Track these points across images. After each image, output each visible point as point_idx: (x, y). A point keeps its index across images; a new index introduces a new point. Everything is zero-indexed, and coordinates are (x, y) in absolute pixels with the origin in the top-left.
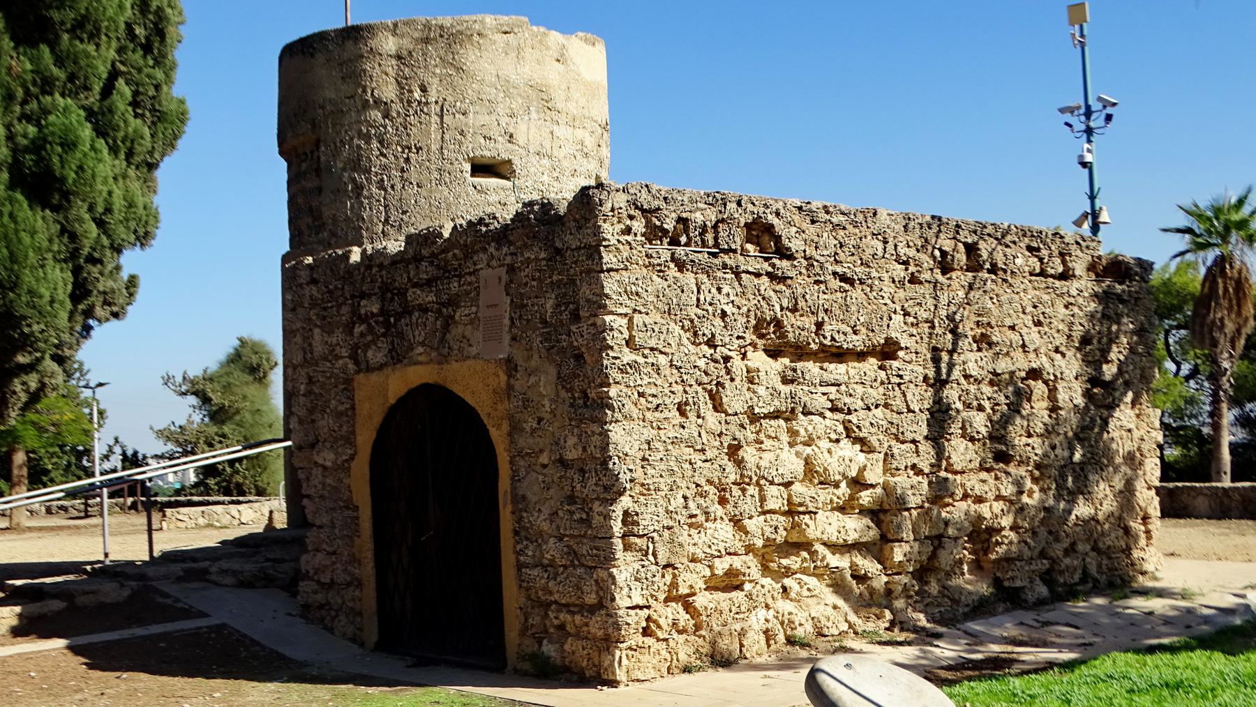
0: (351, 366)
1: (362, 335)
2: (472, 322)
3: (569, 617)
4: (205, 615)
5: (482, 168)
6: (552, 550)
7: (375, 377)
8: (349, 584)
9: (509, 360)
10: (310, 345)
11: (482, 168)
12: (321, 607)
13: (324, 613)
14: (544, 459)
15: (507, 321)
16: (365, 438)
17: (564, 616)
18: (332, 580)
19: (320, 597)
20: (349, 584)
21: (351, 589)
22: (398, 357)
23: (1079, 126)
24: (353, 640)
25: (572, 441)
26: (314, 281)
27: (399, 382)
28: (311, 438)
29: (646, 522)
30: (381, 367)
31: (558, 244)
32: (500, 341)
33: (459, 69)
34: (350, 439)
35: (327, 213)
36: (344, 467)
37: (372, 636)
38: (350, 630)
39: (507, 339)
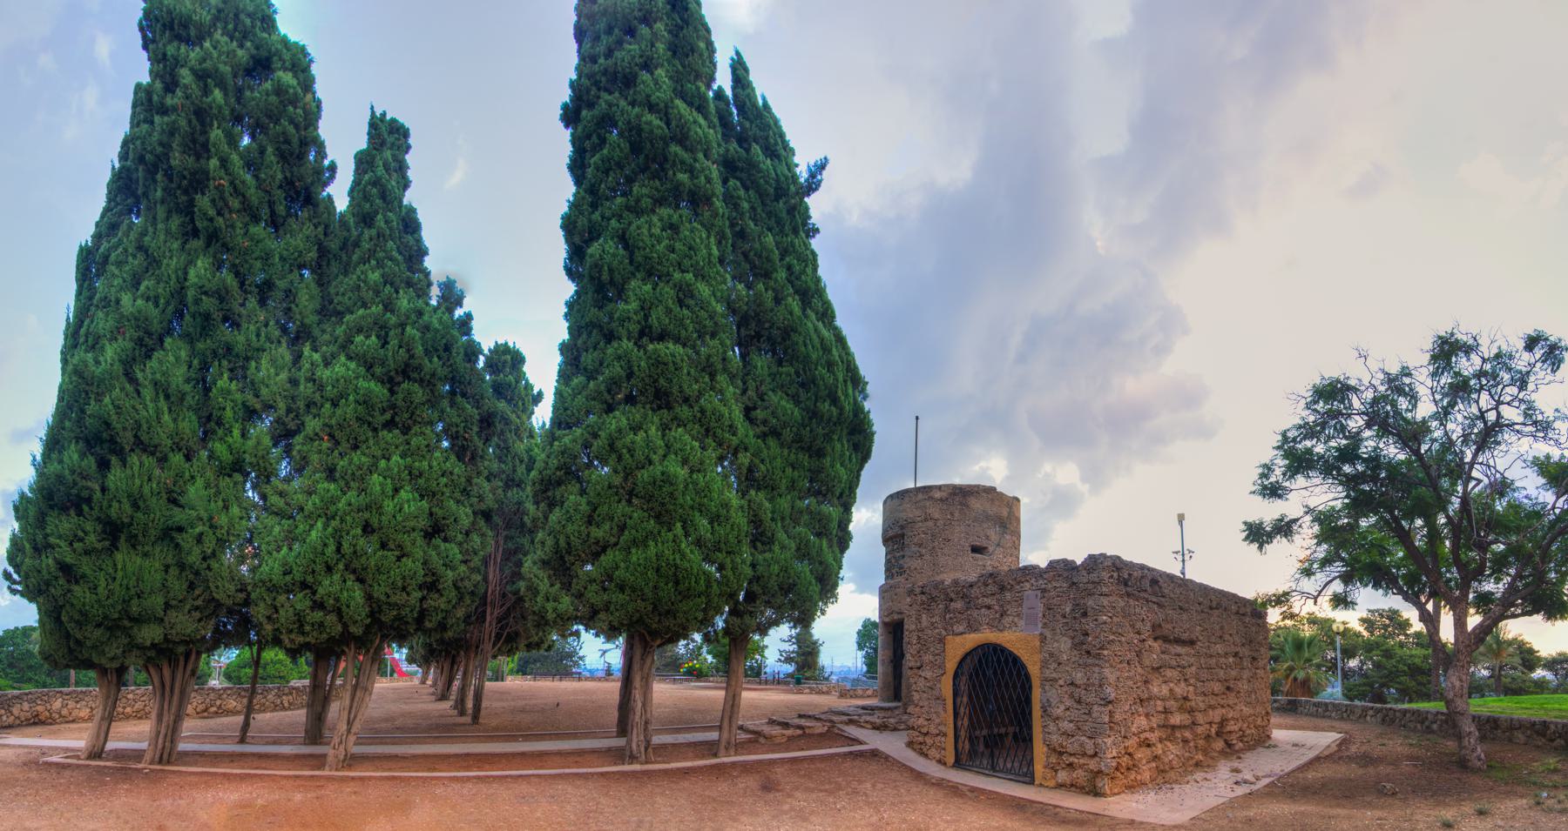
4: (861, 743)
5: (976, 550)
6: (1067, 726)
7: (958, 639)
11: (976, 550)
14: (1061, 682)
16: (951, 666)
17: (1072, 759)
19: (921, 739)
24: (939, 761)
27: (972, 640)
29: (1118, 717)
34: (942, 666)
36: (938, 679)
37: (951, 760)
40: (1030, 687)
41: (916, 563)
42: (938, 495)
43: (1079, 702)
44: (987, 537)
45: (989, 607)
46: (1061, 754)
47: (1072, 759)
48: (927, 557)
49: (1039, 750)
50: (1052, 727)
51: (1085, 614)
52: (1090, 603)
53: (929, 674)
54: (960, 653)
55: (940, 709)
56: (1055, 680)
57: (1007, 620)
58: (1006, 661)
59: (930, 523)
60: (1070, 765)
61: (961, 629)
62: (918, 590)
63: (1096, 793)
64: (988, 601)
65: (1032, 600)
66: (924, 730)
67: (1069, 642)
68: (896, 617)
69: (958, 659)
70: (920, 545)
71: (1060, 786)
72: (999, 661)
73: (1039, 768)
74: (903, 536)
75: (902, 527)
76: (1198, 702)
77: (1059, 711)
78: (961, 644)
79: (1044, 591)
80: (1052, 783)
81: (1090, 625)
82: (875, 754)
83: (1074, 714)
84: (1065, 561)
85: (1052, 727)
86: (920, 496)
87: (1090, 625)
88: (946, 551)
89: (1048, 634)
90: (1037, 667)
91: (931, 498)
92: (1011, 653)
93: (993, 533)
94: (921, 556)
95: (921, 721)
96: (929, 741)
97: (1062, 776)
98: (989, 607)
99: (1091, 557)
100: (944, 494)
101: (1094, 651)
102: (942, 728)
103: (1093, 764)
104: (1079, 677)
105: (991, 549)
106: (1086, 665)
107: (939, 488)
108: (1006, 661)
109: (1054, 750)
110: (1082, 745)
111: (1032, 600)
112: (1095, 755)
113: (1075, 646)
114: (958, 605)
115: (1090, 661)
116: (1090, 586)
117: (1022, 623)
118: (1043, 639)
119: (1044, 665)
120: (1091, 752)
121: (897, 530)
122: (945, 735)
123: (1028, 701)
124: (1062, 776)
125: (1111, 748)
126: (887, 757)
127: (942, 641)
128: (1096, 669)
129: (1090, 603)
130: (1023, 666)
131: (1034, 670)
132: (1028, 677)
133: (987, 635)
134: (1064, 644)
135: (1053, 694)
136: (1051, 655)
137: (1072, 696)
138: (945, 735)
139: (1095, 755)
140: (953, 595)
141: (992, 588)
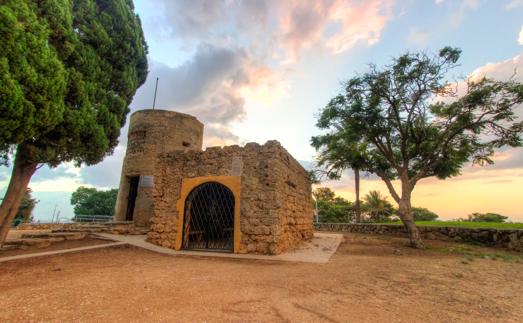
0: (181, 177)
1: (187, 169)
2: (229, 168)
3: (259, 238)
6: (254, 220)
7: (191, 180)
8: (170, 232)
9: (242, 176)
10: (165, 172)
12: (157, 238)
13: (158, 240)
14: (252, 199)
15: (242, 167)
16: (184, 194)
18: (164, 231)
19: (158, 236)
20: (170, 232)
21: (171, 233)
22: (199, 174)
24: (170, 247)
25: (262, 195)
26: (168, 157)
28: (161, 194)
30: (193, 177)
31: (261, 151)
32: (239, 172)
33: (183, 123)
35: (145, 147)
36: (175, 201)
38: (169, 245)
39: (241, 172)
40: (234, 203)
41: (151, 146)
42: (168, 115)
43: (262, 208)
44: (191, 139)
45: (211, 164)
46: (250, 235)
48: (159, 144)
50: (246, 222)
51: (267, 167)
52: (269, 161)
53: (168, 199)
54: (191, 187)
55: (174, 217)
57: (222, 170)
58: (220, 191)
59: (162, 128)
61: (193, 175)
62: (165, 155)
63: (270, 253)
64: (210, 161)
65: (238, 161)
66: (162, 230)
67: (257, 180)
68: (134, 173)
70: (155, 138)
71: (249, 252)
72: (216, 191)
73: (237, 244)
74: (145, 132)
75: (145, 127)
76: (298, 214)
77: (251, 213)
79: (245, 156)
80: (245, 251)
82: (127, 247)
83: (259, 214)
84: (255, 143)
86: (158, 114)
87: (269, 171)
88: (170, 142)
89: (246, 176)
90: (239, 192)
91: (164, 116)
93: (194, 138)
94: (155, 143)
95: (159, 225)
96: (163, 236)
97: (251, 247)
98: (211, 164)
100: (171, 116)
101: (271, 184)
102: (175, 228)
103: (269, 239)
104: (263, 196)
105: (192, 145)
107: (169, 112)
108: (220, 191)
110: (263, 230)
111: (238, 161)
112: (270, 234)
113: (260, 182)
114: (193, 163)
115: (269, 188)
116: (270, 154)
117: (231, 171)
118: (243, 178)
119: (243, 191)
120: (268, 233)
121: (142, 128)
122: (176, 232)
123: (232, 210)
124: (251, 247)
125: (278, 230)
126: (137, 248)
127: (180, 181)
128: (272, 192)
129: (269, 161)
130: (231, 192)
131: (237, 194)
132: (233, 198)
135: (247, 206)
136: (247, 186)
137: (258, 206)
138: (176, 232)
139: (270, 234)
140: (189, 158)
141: (214, 155)
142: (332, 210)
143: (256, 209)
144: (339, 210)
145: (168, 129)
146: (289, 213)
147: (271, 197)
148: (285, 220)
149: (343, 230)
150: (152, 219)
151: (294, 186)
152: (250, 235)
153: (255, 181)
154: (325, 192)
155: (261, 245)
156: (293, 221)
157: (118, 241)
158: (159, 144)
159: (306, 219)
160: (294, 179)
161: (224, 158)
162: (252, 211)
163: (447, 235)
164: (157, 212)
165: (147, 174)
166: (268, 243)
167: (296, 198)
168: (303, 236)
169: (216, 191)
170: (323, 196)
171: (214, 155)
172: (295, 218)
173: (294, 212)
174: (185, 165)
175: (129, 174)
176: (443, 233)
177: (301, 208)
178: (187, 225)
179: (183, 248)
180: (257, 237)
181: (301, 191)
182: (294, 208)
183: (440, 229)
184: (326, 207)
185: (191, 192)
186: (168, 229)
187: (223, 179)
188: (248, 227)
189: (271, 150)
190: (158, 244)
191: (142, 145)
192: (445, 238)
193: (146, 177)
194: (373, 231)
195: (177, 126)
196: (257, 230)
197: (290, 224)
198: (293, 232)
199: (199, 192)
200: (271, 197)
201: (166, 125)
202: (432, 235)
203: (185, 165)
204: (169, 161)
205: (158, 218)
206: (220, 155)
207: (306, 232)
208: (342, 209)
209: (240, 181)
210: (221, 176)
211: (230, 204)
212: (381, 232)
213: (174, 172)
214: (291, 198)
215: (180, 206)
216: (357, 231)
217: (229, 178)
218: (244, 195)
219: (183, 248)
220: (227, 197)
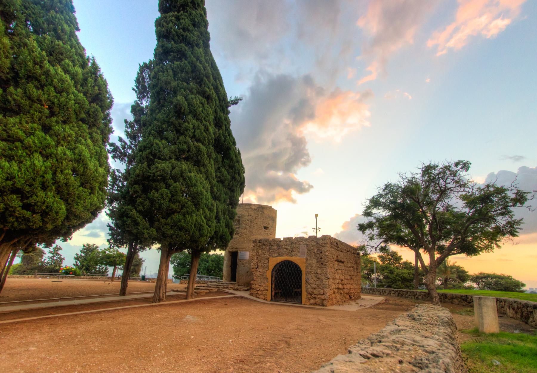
5: (265, 228)
6: (314, 286)
7: (274, 258)
11: (265, 228)
16: (271, 267)
19: (256, 292)
22: (280, 255)
23: (315, 231)
27: (280, 259)
34: (267, 268)
36: (265, 272)
37: (269, 298)
40: (302, 274)
42: (253, 207)
43: (319, 278)
44: (269, 224)
45: (287, 249)
46: (311, 295)
47: (315, 296)
48: (249, 229)
49: (304, 294)
50: (309, 286)
51: (321, 252)
53: (261, 270)
54: (275, 263)
55: (266, 281)
56: (311, 272)
57: (294, 253)
58: (293, 266)
59: (250, 217)
60: (315, 298)
61: (276, 255)
62: (258, 241)
63: (323, 305)
64: (287, 247)
65: (303, 247)
67: (316, 260)
68: (234, 250)
69: (274, 265)
71: (311, 304)
72: (290, 266)
73: (304, 299)
74: (239, 220)
76: (345, 282)
77: (312, 281)
78: (275, 260)
79: (308, 245)
80: (308, 303)
81: (323, 255)
82: (242, 297)
83: (317, 282)
85: (309, 286)
86: (247, 207)
87: (323, 255)
88: (255, 227)
89: (309, 258)
90: (305, 268)
92: (295, 264)
94: (246, 228)
95: (257, 286)
96: (259, 292)
97: (312, 301)
98: (287, 249)
99: (323, 236)
100: (255, 207)
102: (267, 288)
103: (323, 297)
104: (319, 271)
105: (270, 228)
106: (321, 268)
108: (293, 266)
109: (309, 293)
110: (319, 291)
112: (323, 294)
113: (318, 262)
114: (275, 247)
115: (323, 266)
117: (299, 254)
118: (307, 259)
119: (307, 267)
122: (267, 290)
123: (301, 279)
124: (312, 301)
125: (328, 292)
126: (247, 298)
127: (268, 259)
129: (323, 249)
130: (299, 268)
131: (303, 269)
132: (301, 271)
133: (285, 258)
134: (314, 261)
135: (309, 276)
136: (309, 264)
137: (316, 277)
138: (267, 290)
141: (288, 243)
142: (397, 275)
143: (315, 279)
144: (405, 275)
145: (254, 217)
146: (337, 281)
147: (324, 271)
148: (334, 286)
149: (392, 294)
150: (252, 282)
151: (343, 262)
152: (311, 295)
153: (314, 262)
154: (392, 256)
155: (318, 301)
156: (341, 286)
157: (234, 294)
158: (249, 229)
159: (354, 285)
160: (342, 257)
161: (294, 246)
162: (313, 280)
163: (466, 301)
164: (255, 278)
165: (243, 251)
166: (322, 299)
167: (344, 271)
168: (350, 297)
169: (290, 266)
170: (390, 260)
171: (288, 243)
172: (342, 284)
173: (342, 280)
174: (270, 249)
175: (231, 250)
176: (463, 300)
177: (349, 277)
178: (273, 286)
179: (272, 300)
180: (315, 296)
181: (349, 265)
182: (342, 277)
183: (462, 296)
184: (391, 272)
185: (275, 266)
186: (262, 289)
187: (293, 259)
188: (310, 290)
189: (324, 241)
190: (256, 297)
191: (238, 230)
192: (465, 303)
193: (242, 252)
194: (414, 296)
195: (260, 215)
196: (316, 292)
197: (338, 288)
198: (341, 294)
199: (280, 266)
200: (324, 271)
201: (253, 215)
202: (456, 301)
203: (270, 249)
204: (260, 246)
205: (256, 282)
206: (292, 243)
207: (352, 294)
208: (409, 274)
209: (305, 261)
210: (293, 257)
211: (299, 274)
212: (420, 297)
213: (264, 253)
214: (339, 271)
215: (269, 274)
216: (402, 295)
217: (298, 259)
218: (308, 270)
219: (272, 300)
220: (297, 270)
